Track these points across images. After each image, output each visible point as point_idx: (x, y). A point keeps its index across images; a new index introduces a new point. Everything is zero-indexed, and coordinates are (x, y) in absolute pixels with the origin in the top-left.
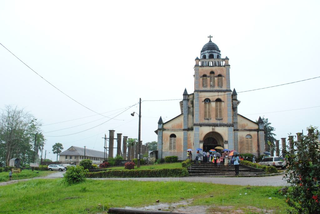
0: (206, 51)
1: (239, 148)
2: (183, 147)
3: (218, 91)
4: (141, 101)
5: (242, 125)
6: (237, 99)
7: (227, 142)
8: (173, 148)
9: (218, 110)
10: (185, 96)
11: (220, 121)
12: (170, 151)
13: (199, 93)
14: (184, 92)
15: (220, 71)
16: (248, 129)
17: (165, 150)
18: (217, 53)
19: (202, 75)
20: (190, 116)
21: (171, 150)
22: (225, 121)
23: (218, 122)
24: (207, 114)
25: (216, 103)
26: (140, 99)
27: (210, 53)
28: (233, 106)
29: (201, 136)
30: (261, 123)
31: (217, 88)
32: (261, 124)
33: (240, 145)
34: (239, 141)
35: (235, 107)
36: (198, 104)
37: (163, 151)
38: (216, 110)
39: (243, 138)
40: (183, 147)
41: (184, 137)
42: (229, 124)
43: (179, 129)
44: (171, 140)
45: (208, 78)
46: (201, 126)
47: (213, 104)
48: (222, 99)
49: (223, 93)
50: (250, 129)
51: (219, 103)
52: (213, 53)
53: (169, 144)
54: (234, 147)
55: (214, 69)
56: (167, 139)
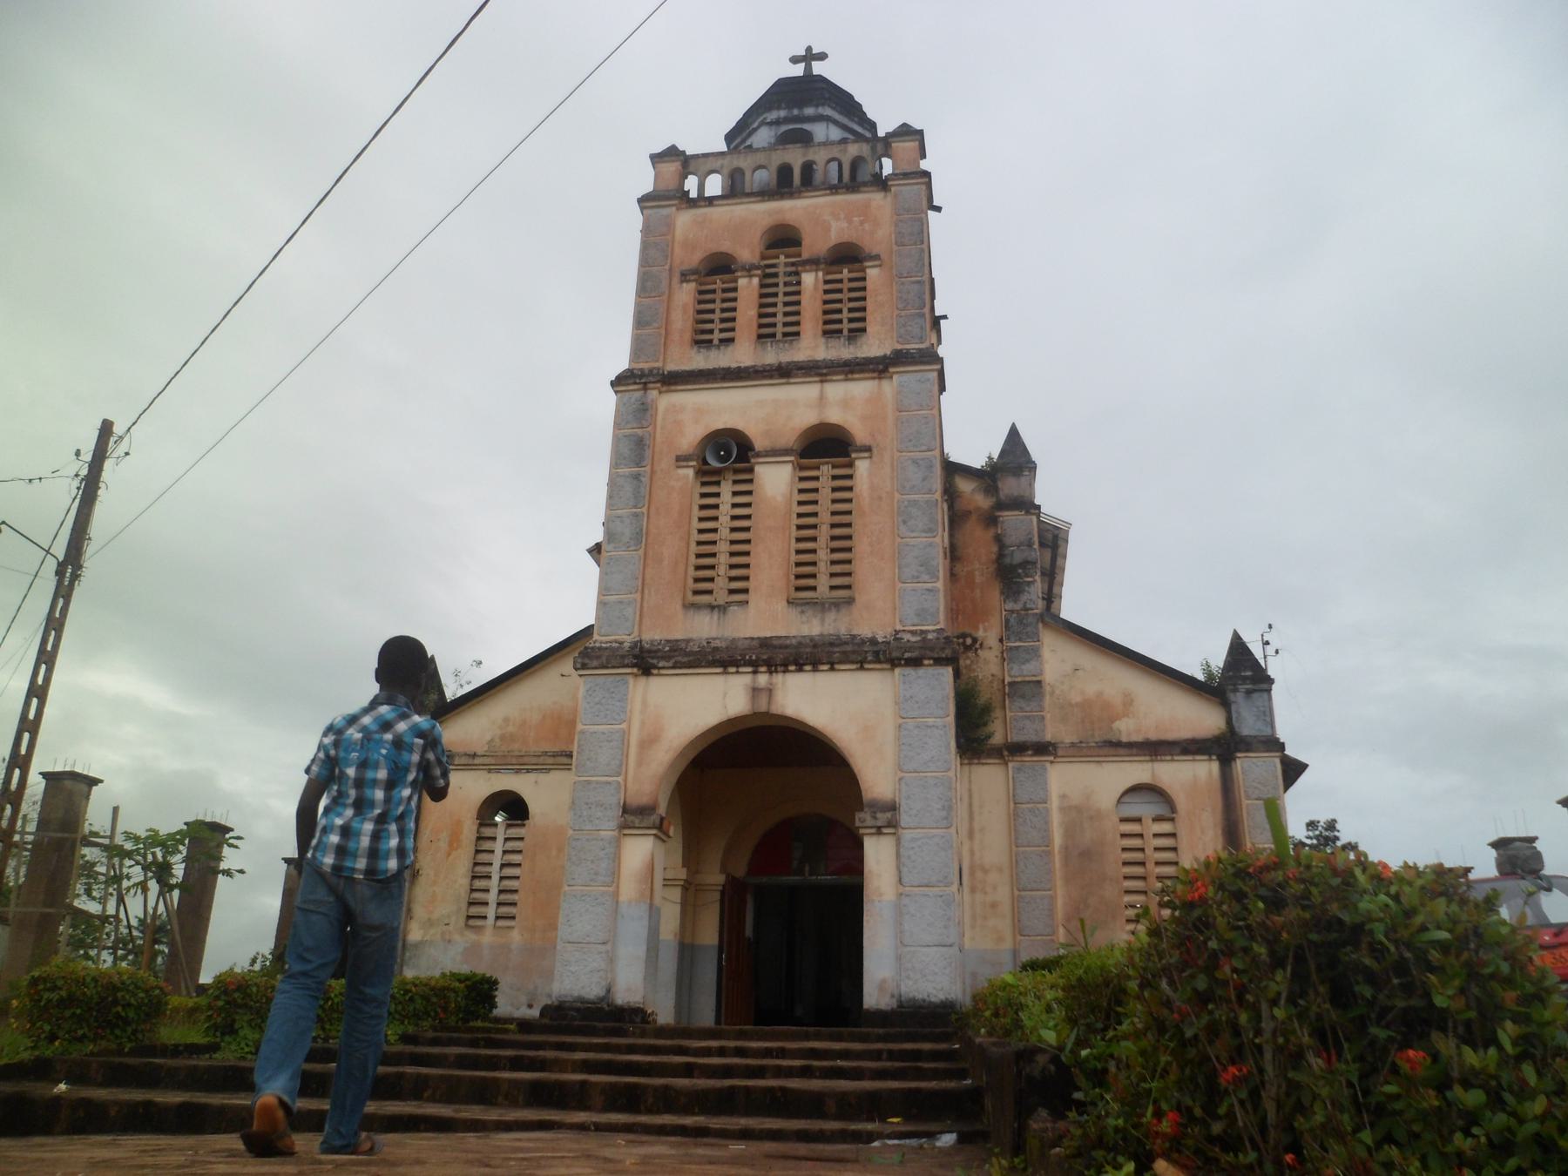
1: (1060, 902)
5: (1086, 705)
6: (1037, 502)
8: (491, 912)
9: (824, 533)
11: (831, 616)
12: (471, 936)
15: (846, 225)
17: (430, 923)
18: (836, 123)
19: (695, 259)
21: (479, 929)
23: (811, 627)
24: (722, 570)
25: (802, 468)
27: (784, 128)
28: (1001, 556)
29: (640, 763)
30: (1245, 679)
31: (811, 347)
34: (1058, 840)
35: (1018, 558)
36: (637, 477)
38: (806, 527)
39: (1097, 816)
42: (913, 639)
44: (487, 845)
46: (647, 670)
48: (860, 434)
49: (861, 388)
50: (1153, 736)
51: (826, 470)
52: (806, 126)
53: (462, 881)
55: (793, 209)
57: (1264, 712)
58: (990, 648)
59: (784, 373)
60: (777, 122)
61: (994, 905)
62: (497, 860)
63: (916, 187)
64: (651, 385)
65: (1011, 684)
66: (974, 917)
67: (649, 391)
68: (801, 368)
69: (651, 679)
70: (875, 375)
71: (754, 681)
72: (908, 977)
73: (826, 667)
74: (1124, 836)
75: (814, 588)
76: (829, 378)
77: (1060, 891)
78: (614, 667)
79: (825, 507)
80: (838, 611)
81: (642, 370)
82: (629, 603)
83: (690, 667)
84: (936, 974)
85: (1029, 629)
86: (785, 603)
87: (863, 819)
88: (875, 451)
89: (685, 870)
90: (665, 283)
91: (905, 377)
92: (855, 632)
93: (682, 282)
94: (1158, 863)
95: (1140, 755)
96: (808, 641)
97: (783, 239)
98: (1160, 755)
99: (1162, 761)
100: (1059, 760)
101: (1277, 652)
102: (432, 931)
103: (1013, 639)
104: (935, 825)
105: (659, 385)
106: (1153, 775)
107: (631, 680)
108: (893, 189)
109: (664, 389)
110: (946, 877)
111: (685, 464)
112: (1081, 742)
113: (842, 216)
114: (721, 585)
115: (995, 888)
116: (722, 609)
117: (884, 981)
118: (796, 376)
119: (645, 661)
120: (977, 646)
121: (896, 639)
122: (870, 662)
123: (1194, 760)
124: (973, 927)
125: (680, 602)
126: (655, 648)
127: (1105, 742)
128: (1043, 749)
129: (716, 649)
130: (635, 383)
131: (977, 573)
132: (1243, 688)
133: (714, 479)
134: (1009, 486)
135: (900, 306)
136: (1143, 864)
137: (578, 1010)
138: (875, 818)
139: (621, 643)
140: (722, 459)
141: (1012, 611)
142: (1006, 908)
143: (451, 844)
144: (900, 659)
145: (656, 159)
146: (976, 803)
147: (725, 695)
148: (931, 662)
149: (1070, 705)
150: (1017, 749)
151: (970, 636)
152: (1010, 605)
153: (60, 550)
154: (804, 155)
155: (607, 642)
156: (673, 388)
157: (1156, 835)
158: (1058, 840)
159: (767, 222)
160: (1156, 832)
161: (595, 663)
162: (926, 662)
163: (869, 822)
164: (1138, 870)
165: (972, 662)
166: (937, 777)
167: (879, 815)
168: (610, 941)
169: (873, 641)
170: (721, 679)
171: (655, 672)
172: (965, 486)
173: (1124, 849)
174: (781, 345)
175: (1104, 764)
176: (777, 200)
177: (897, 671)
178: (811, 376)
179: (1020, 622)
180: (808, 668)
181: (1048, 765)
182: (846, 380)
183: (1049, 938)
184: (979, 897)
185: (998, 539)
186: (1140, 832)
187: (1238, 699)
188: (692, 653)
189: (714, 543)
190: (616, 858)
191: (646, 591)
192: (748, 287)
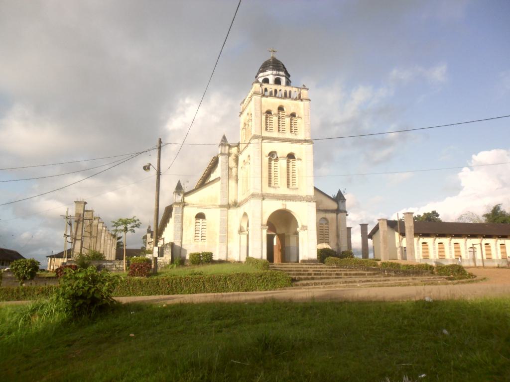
0: (269, 72)
2: (220, 236)
3: (291, 141)
4: (162, 145)
7: (305, 228)
8: (200, 238)
10: (223, 148)
11: (295, 191)
14: (222, 141)
16: (323, 209)
20: (232, 183)
21: (197, 241)
26: (160, 140)
31: (288, 135)
37: (183, 243)
40: (218, 237)
41: (221, 219)
43: (213, 205)
44: (198, 224)
50: (325, 209)
52: (281, 77)
53: (193, 232)
56: (190, 222)
60: (275, 75)
62: (200, 227)
97: (281, 109)
129: (276, 196)
132: (341, 201)
153: (156, 168)
164: (322, 233)
169: (302, 197)
187: (340, 203)
188: (271, 197)
192: (275, 119)
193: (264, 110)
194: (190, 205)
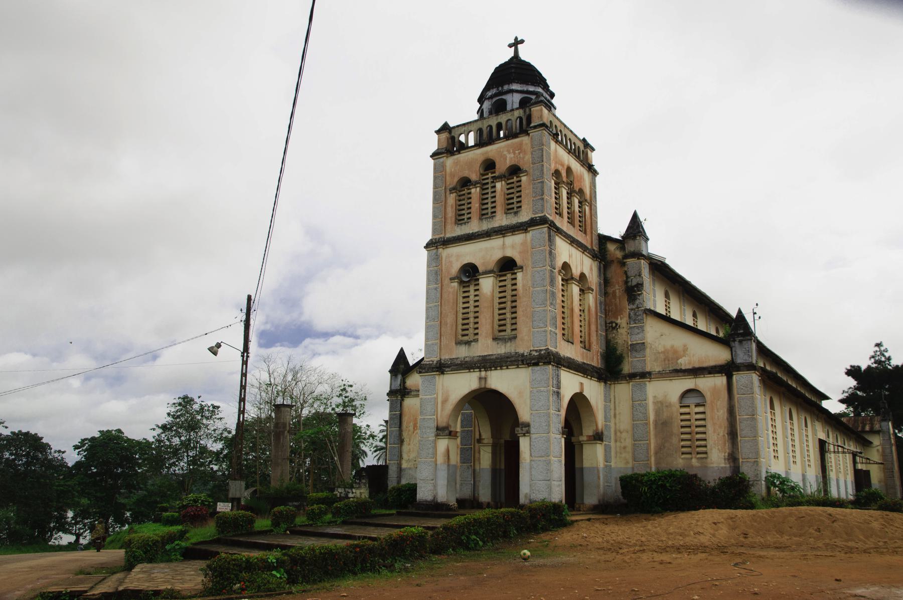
11: (509, 344)
13: (440, 250)
15: (512, 155)
16: (690, 367)
17: (408, 461)
22: (523, 347)
23: (501, 350)
25: (501, 276)
27: (494, 100)
28: (626, 282)
29: (442, 410)
30: (739, 335)
31: (502, 220)
32: (740, 342)
33: (656, 436)
35: (634, 283)
36: (436, 289)
37: (404, 465)
39: (669, 406)
42: (536, 354)
45: (473, 190)
46: (443, 373)
47: (487, 284)
48: (519, 262)
50: (697, 365)
52: (504, 97)
54: (634, 445)
55: (491, 150)
57: (748, 350)
58: (623, 328)
59: (487, 235)
61: (625, 448)
63: (540, 132)
64: (439, 247)
65: (631, 345)
66: (616, 453)
67: (439, 249)
68: (495, 232)
69: (445, 375)
70: (523, 231)
71: (480, 375)
72: (534, 493)
73: (505, 368)
74: (681, 414)
75: (505, 331)
76: (506, 235)
77: (653, 441)
78: (430, 372)
79: (509, 293)
80: (511, 342)
81: (436, 239)
82: (436, 344)
83: (457, 370)
84: (543, 491)
85: (639, 317)
86: (492, 339)
87: (518, 430)
88: (524, 267)
89: (492, 439)
90: (443, 195)
91: (535, 232)
92: (517, 351)
93: (450, 193)
94: (697, 426)
95: (689, 376)
96: (499, 356)
97: (489, 165)
98: (699, 375)
99: (699, 377)
100: (652, 380)
101: (760, 318)
102: (410, 464)
103: (632, 323)
104: (543, 432)
105: (441, 246)
106: (696, 385)
107: (437, 377)
108: (531, 134)
109: (445, 247)
110: (547, 453)
111: (453, 281)
112: (663, 371)
113: (511, 151)
114: (471, 331)
115: (625, 440)
116: (468, 343)
117: (527, 494)
118: (493, 236)
119: (441, 368)
120: (618, 327)
121: (530, 354)
122: (520, 365)
123: (714, 376)
124: (616, 457)
125: (454, 342)
126: (445, 363)
127: (674, 370)
128: (645, 375)
130: (433, 247)
131: (617, 291)
132: (738, 339)
133: (467, 284)
134: (631, 246)
135: (534, 195)
136: (690, 427)
137: (424, 504)
138: (522, 430)
139: (433, 361)
140: (468, 277)
141: (632, 309)
142: (629, 449)
143: (414, 428)
144: (530, 363)
145: (438, 132)
146: (617, 403)
147: (470, 381)
148: (542, 364)
149: (659, 353)
150: (632, 376)
151: (615, 322)
152: (631, 306)
154: (497, 119)
155: (428, 362)
156: (448, 246)
157: (696, 413)
158: (652, 417)
159: (482, 159)
160: (696, 412)
161: (424, 371)
162: (540, 364)
163: (520, 432)
165: (615, 335)
166: (544, 413)
167: (523, 429)
168: (435, 479)
169: (523, 355)
170: (469, 374)
171: (445, 373)
172: (611, 247)
173: (682, 420)
174: (489, 220)
175: (673, 381)
176: (486, 146)
177: (530, 368)
178: (498, 235)
179: (635, 314)
180: (499, 368)
181: (647, 383)
182: (513, 235)
183: (647, 462)
184: (618, 444)
185: (626, 273)
186: (689, 412)
188: (457, 365)
189: (468, 313)
190: (435, 448)
191: (442, 338)
192: (475, 191)
193: (453, 182)
194: (413, 393)
